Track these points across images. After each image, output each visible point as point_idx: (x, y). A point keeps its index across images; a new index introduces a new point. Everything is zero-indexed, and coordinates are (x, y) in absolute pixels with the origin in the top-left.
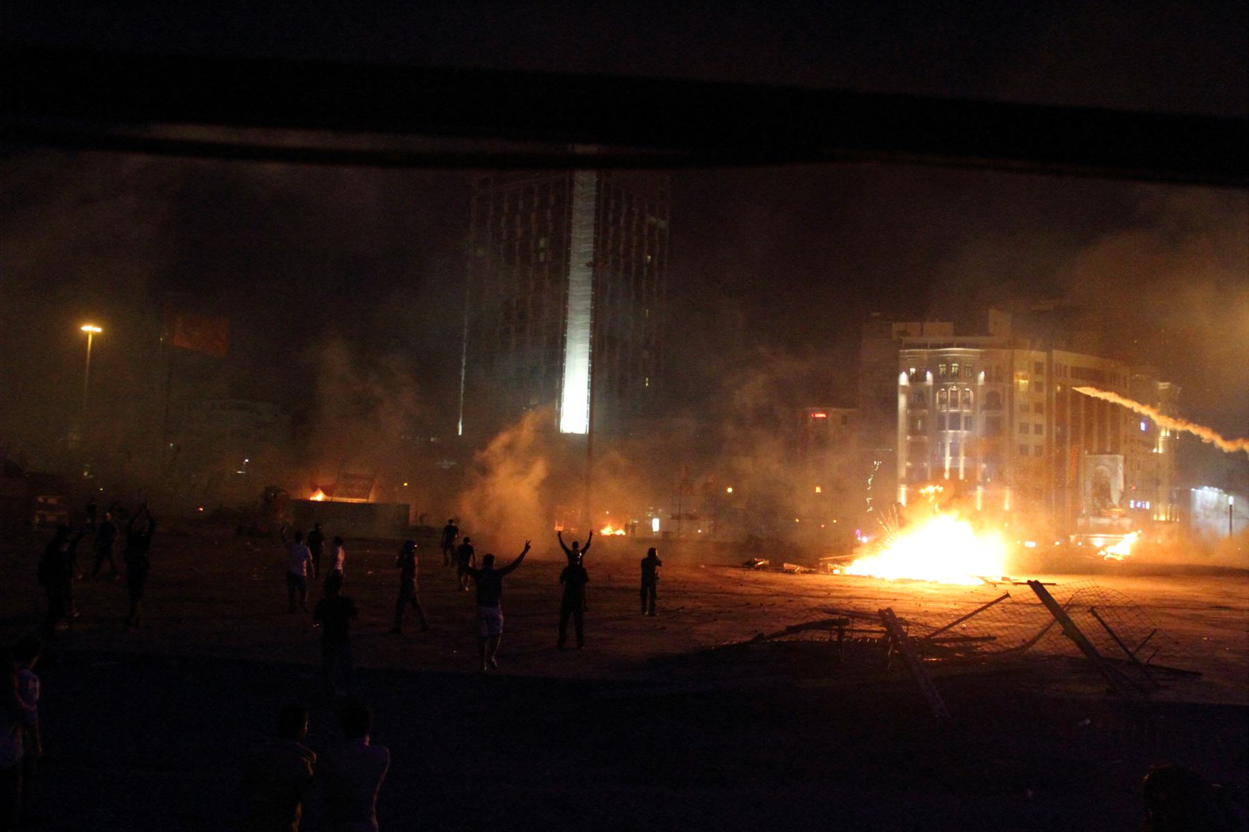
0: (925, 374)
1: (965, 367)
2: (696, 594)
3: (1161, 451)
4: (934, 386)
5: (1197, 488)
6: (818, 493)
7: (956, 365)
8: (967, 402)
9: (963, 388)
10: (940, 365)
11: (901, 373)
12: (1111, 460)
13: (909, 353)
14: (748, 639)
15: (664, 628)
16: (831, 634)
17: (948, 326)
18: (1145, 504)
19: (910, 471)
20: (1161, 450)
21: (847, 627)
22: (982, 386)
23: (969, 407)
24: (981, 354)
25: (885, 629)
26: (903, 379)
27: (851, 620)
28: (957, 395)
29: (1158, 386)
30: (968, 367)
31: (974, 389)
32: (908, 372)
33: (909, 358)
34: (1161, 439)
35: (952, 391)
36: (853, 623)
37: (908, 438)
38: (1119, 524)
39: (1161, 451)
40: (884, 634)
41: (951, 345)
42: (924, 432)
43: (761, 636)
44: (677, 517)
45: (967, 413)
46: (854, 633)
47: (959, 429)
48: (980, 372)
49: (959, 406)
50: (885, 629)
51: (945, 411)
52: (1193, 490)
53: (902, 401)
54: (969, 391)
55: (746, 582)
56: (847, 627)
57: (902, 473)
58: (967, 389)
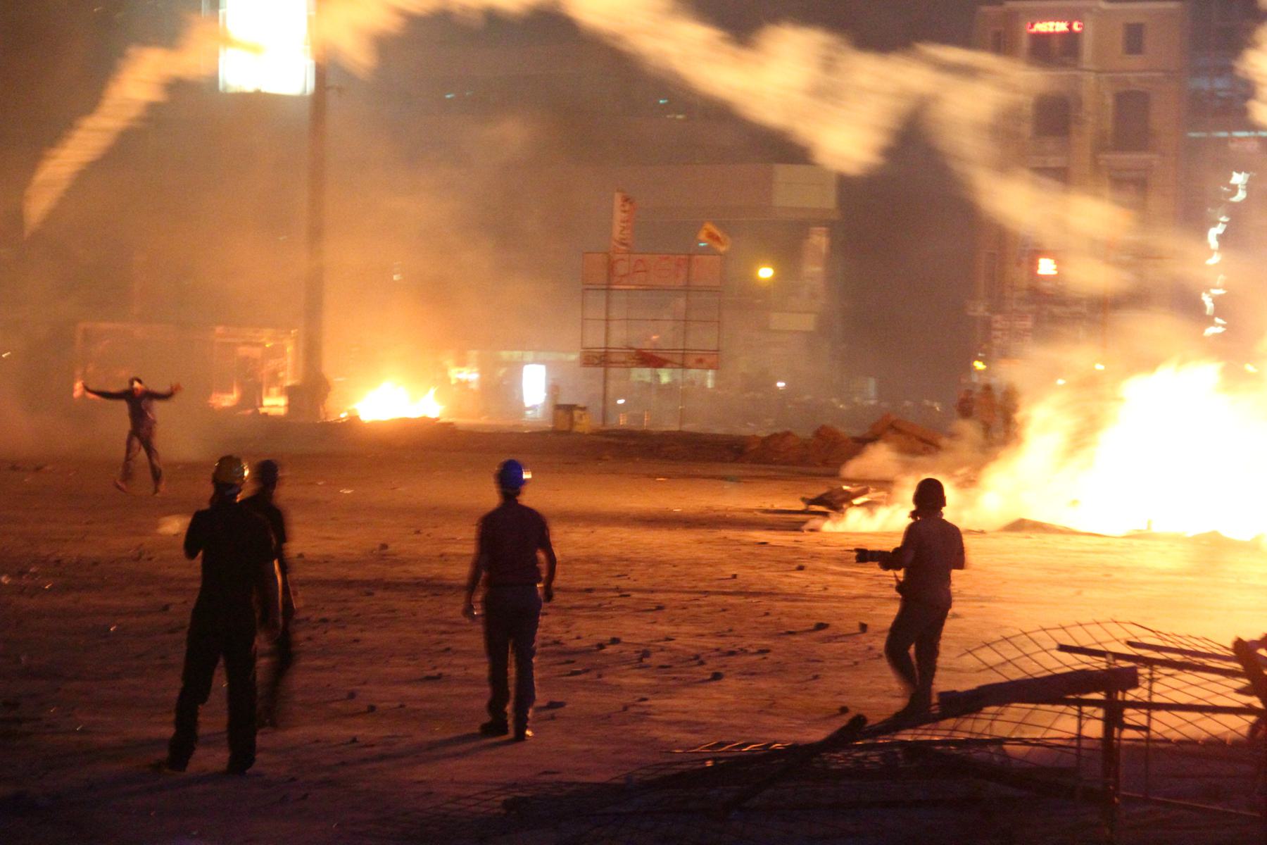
2: (660, 597)
14: (817, 734)
15: (552, 705)
16: (1080, 716)
21: (1131, 695)
25: (1256, 702)
27: (1144, 671)
36: (1152, 680)
40: (1252, 719)
43: (859, 720)
44: (599, 360)
46: (1156, 714)
50: (1256, 702)
55: (815, 556)
56: (1131, 695)
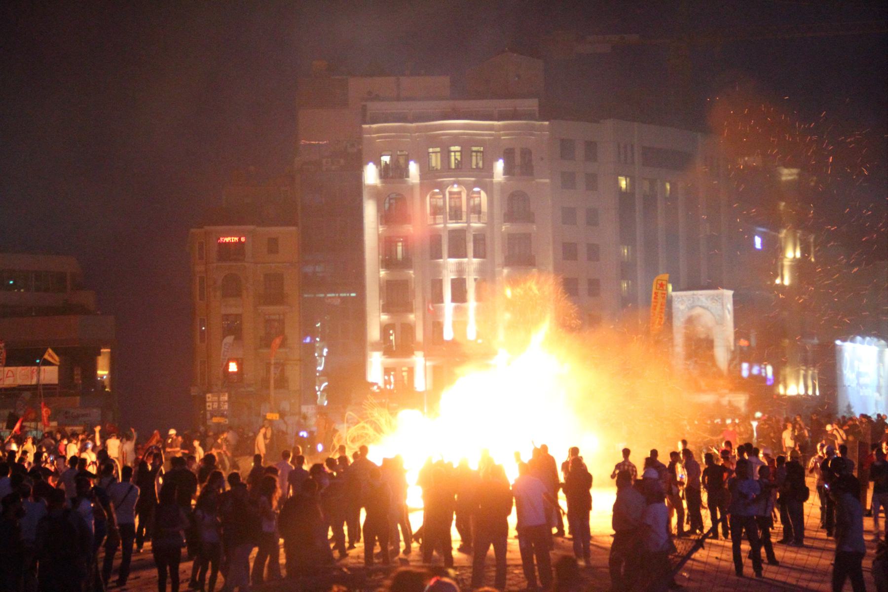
0: (407, 165)
3: (787, 282)
4: (422, 184)
5: (844, 340)
6: (233, 373)
7: (457, 148)
8: (476, 210)
9: (469, 187)
10: (431, 150)
11: (367, 164)
12: (713, 298)
13: (378, 131)
17: (444, 81)
18: (765, 368)
19: (385, 330)
20: (786, 279)
22: (500, 183)
23: (479, 220)
26: (371, 175)
28: (460, 198)
29: (781, 175)
30: (477, 152)
31: (488, 188)
32: (378, 163)
33: (379, 138)
34: (787, 263)
35: (451, 193)
37: (383, 273)
38: (730, 402)
39: (787, 282)
42: (406, 263)
45: (477, 229)
47: (465, 256)
48: (497, 160)
49: (464, 218)
51: (442, 226)
52: (838, 342)
53: (370, 211)
54: (479, 193)
57: (374, 333)
58: (476, 189)
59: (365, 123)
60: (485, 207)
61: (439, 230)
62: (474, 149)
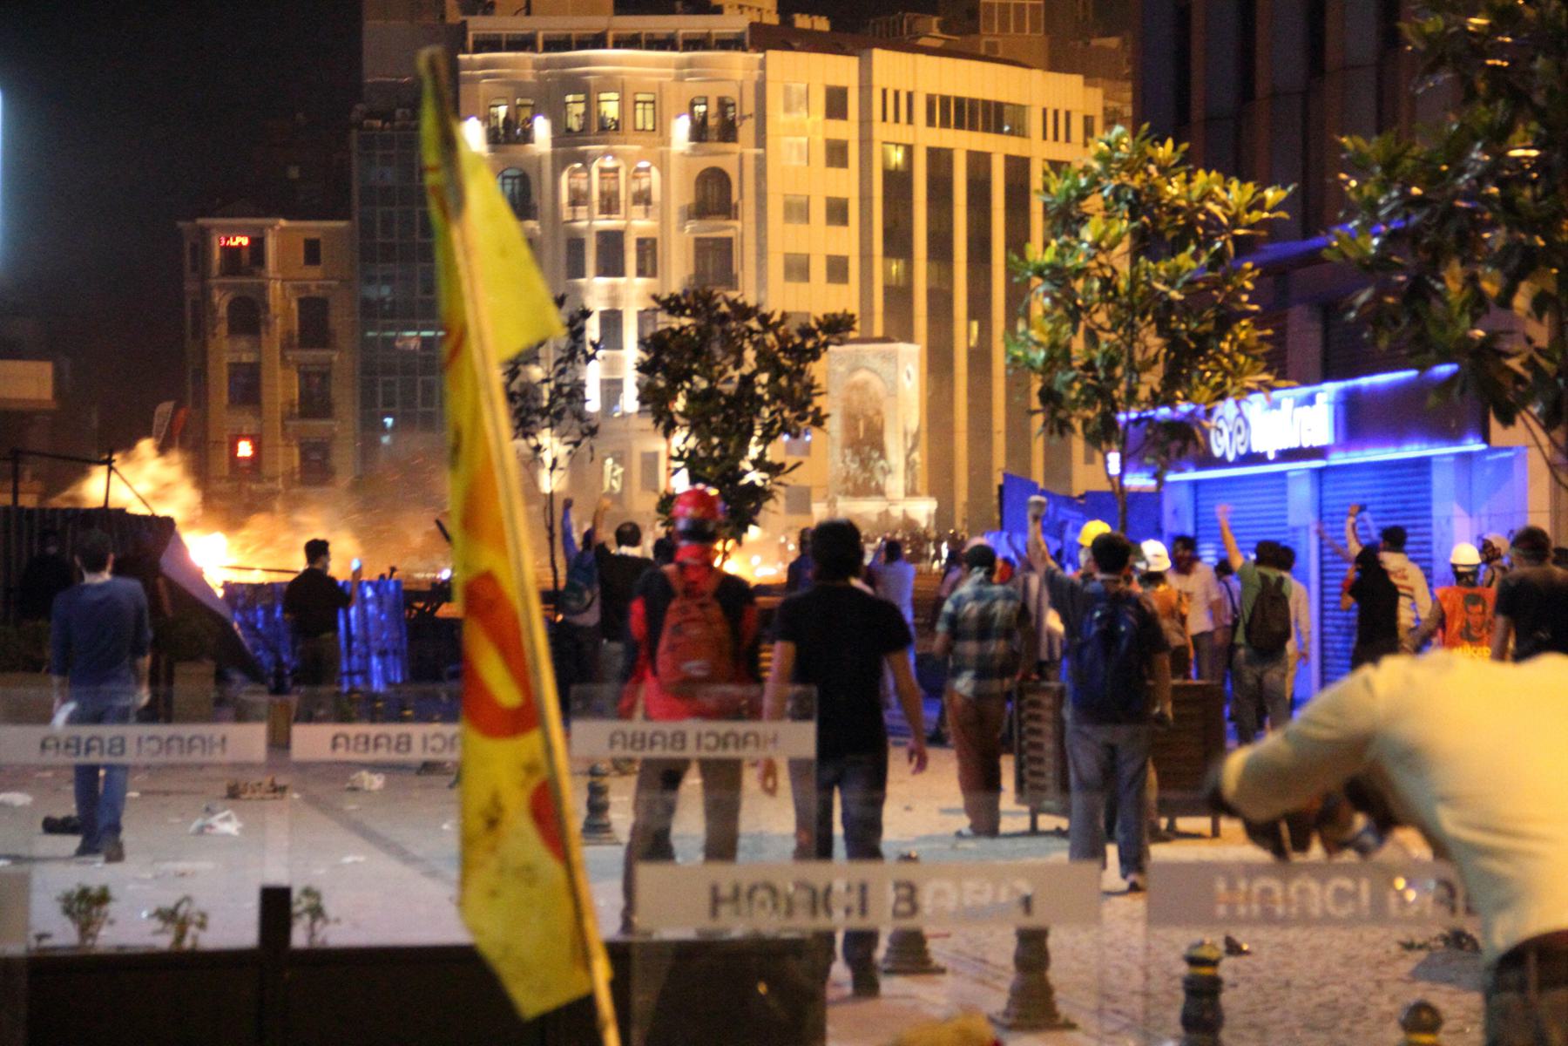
1: (636, 102)
4: (554, 155)
8: (643, 198)
10: (570, 98)
24: (680, 65)
30: (645, 102)
31: (662, 163)
35: (602, 171)
41: (598, 41)
48: (678, 116)
54: (648, 170)
59: (465, 52)
60: (656, 196)
61: (582, 231)
62: (640, 97)
